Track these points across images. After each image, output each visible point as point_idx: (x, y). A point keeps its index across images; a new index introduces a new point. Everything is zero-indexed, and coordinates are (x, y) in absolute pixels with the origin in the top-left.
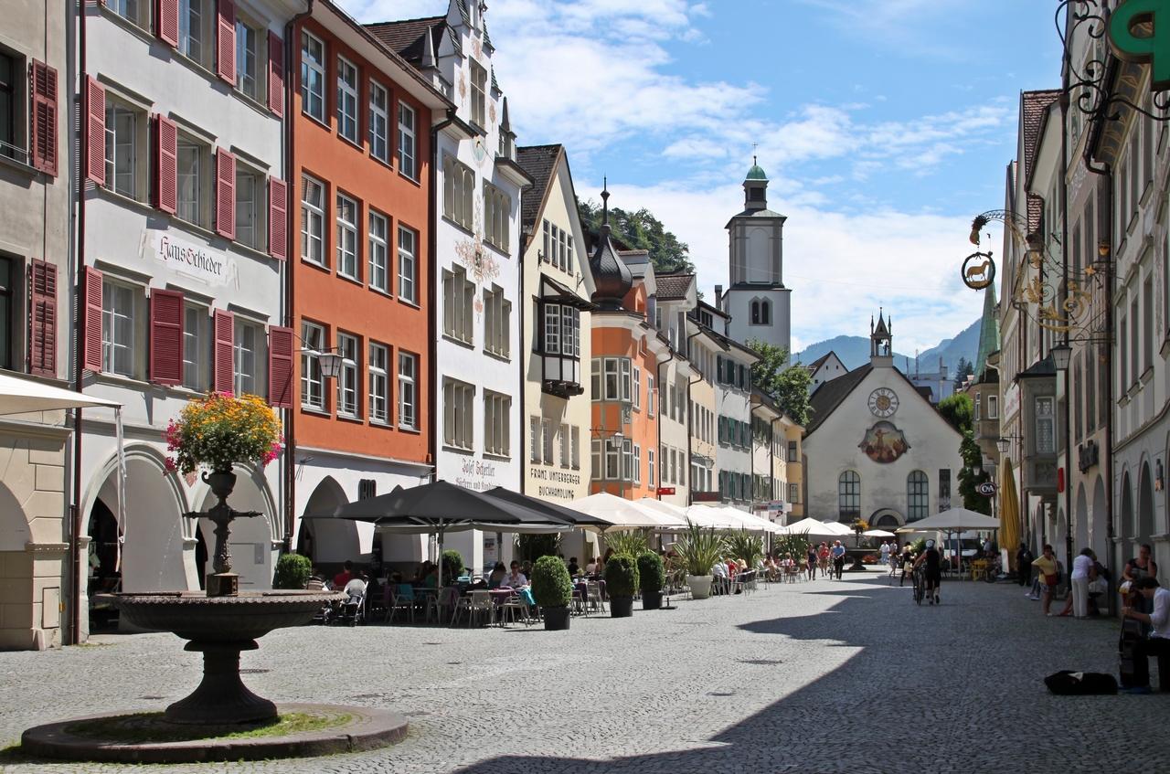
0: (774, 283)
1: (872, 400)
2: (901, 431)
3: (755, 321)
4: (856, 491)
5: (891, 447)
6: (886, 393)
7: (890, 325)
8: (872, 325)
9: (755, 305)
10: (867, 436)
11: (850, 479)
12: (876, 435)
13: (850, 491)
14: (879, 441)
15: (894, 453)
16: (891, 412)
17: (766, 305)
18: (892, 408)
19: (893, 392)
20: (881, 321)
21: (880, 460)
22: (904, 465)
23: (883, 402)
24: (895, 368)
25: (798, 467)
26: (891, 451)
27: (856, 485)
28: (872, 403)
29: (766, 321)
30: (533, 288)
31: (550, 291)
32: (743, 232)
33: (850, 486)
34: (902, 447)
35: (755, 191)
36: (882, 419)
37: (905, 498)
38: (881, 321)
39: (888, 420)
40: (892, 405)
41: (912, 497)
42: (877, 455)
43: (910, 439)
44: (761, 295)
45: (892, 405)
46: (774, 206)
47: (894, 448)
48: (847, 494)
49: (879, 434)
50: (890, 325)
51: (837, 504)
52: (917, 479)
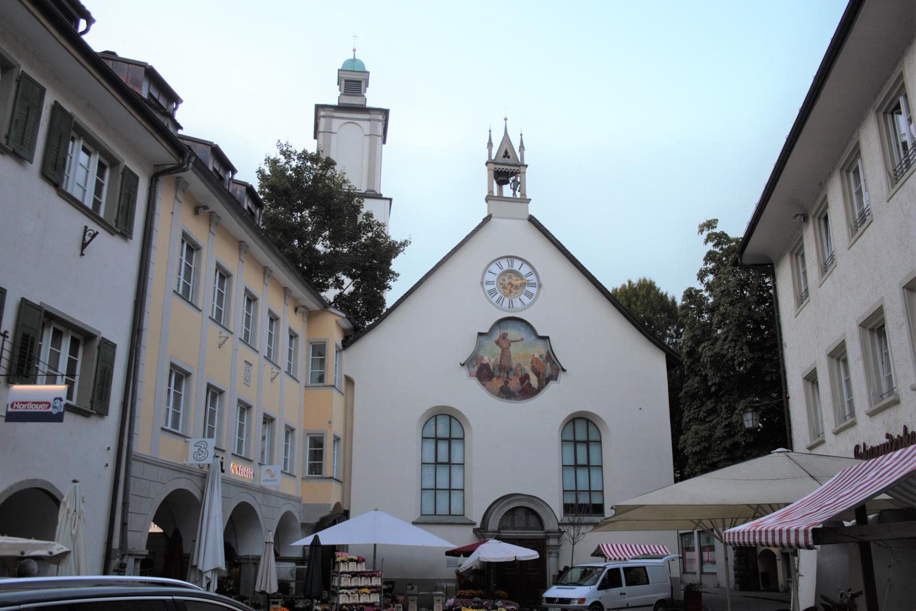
1: (489, 277)
2: (546, 338)
4: (456, 458)
5: (528, 369)
6: (517, 265)
7: (522, 147)
8: (490, 144)
10: (479, 346)
12: (497, 343)
13: (443, 457)
14: (502, 355)
15: (534, 381)
18: (529, 295)
20: (506, 139)
21: (506, 393)
22: (555, 403)
23: (512, 283)
24: (532, 220)
26: (527, 377)
27: (456, 447)
28: (488, 283)
34: (549, 370)
35: (353, 81)
38: (506, 139)
41: (570, 474)
42: (497, 383)
46: (373, 98)
50: (522, 147)
52: (582, 431)
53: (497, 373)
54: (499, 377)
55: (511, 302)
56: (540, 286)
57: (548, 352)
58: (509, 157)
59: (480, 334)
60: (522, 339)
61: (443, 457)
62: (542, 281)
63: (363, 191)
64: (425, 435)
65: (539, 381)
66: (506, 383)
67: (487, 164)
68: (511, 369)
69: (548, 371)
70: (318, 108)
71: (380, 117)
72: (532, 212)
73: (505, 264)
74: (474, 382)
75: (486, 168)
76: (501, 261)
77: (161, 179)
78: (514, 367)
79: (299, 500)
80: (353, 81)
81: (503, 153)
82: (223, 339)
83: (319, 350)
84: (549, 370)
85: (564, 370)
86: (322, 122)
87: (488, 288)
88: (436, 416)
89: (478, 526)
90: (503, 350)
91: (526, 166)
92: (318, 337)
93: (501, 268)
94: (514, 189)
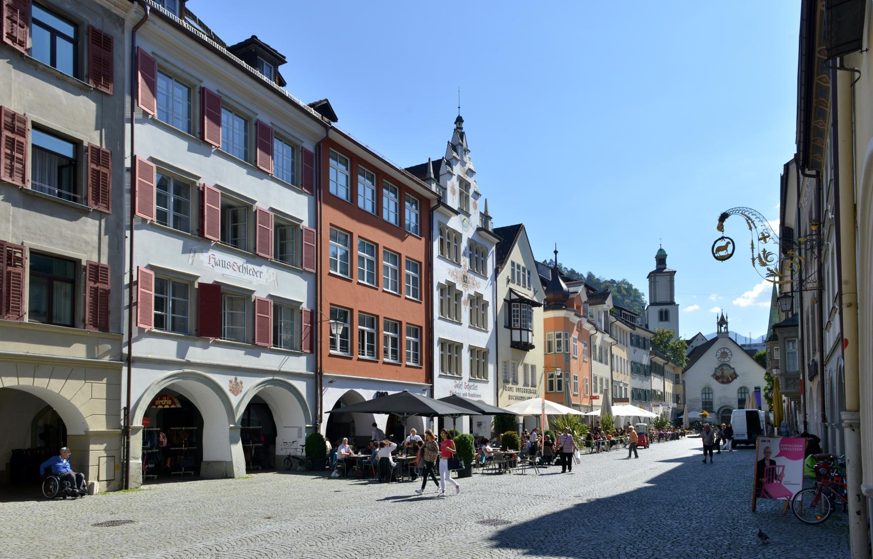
3: (661, 319)
9: (661, 312)
17: (667, 312)
21: (723, 382)
22: (736, 384)
23: (724, 354)
25: (681, 387)
29: (667, 319)
30: (503, 294)
31: (514, 297)
32: (655, 279)
34: (735, 376)
35: (661, 259)
43: (738, 373)
44: (664, 308)
46: (670, 266)
49: (722, 370)
74: (715, 381)
80: (661, 259)
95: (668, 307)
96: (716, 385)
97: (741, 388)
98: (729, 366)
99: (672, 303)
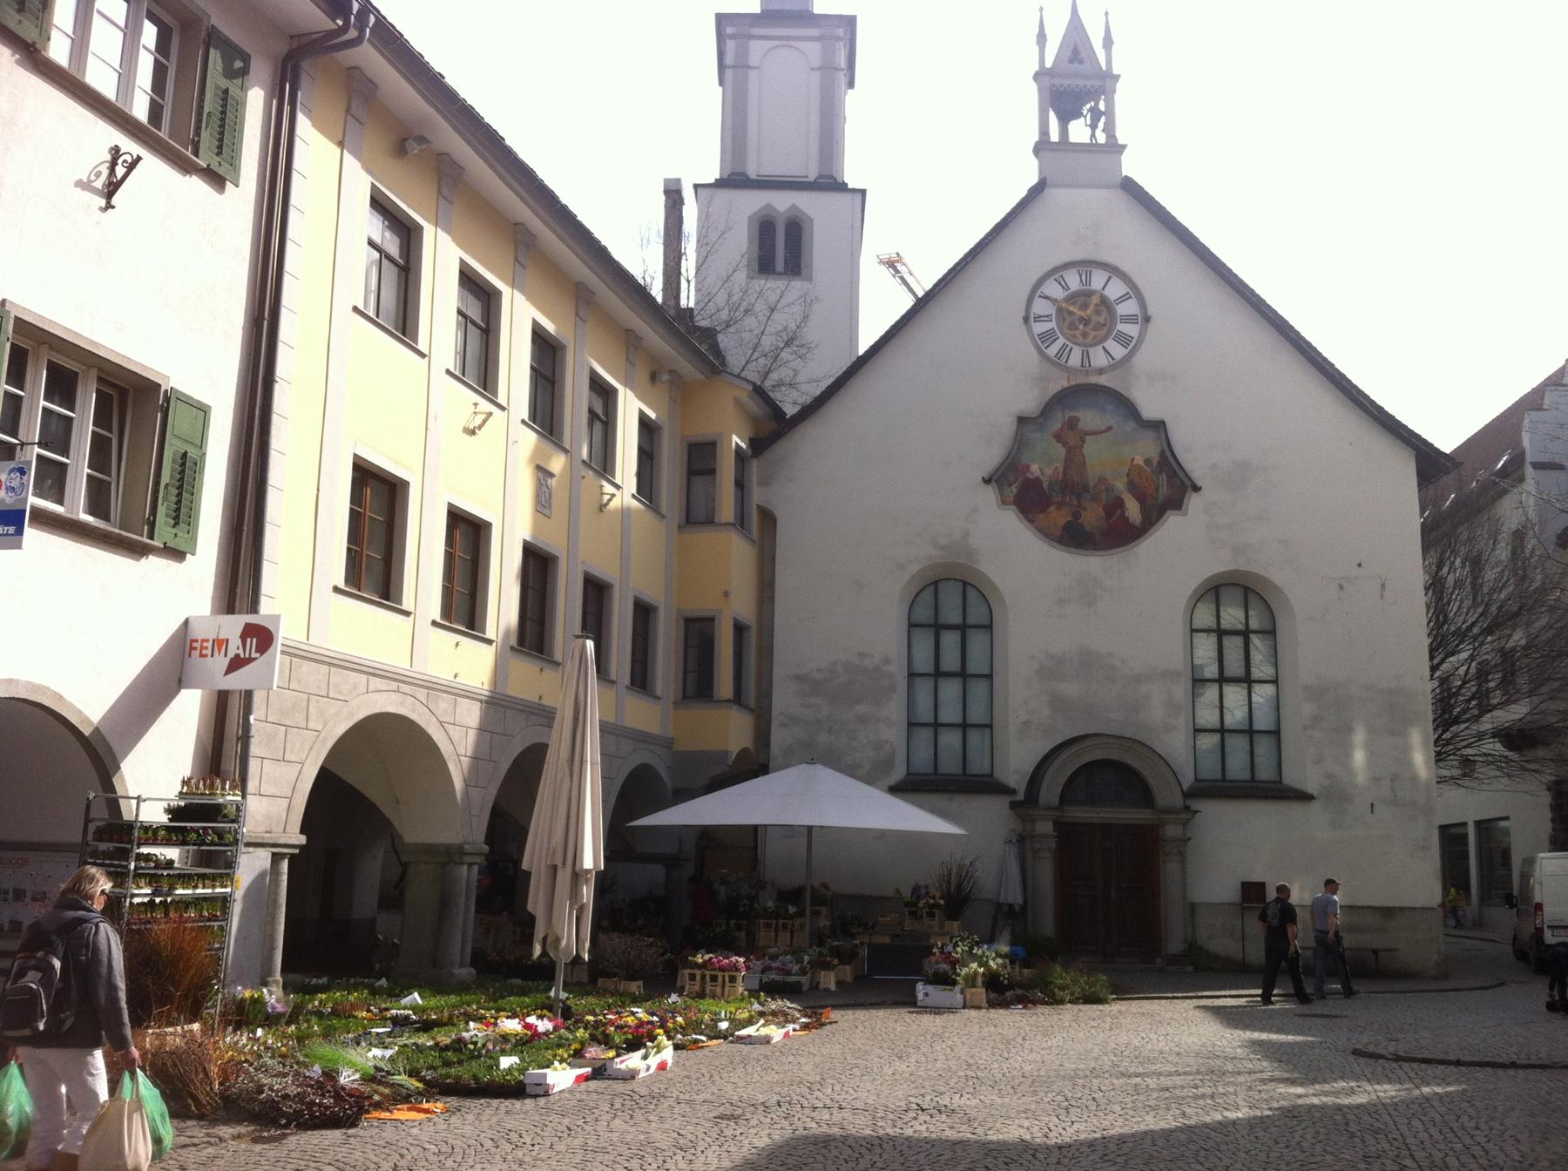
0: (820, 177)
1: (1040, 307)
2: (1159, 426)
4: (976, 664)
5: (1120, 486)
6: (1098, 280)
8: (1042, 38)
9: (765, 228)
11: (951, 615)
12: (1058, 437)
13: (950, 661)
14: (1068, 460)
15: (1133, 510)
16: (1118, 351)
17: (796, 230)
18: (1124, 339)
19: (1125, 277)
20: (1076, 26)
21: (1074, 538)
24: (1131, 188)
26: (1119, 503)
28: (1038, 319)
32: (743, 53)
33: (950, 640)
34: (1167, 487)
36: (1081, 380)
37: (1181, 690)
38: (1076, 26)
39: (1103, 380)
40: (1121, 327)
42: (1058, 518)
43: (1194, 462)
44: (782, 202)
45: (1121, 327)
47: (1132, 488)
48: (938, 674)
50: (1108, 42)
51: (895, 710)
53: (1057, 498)
54: (1060, 506)
55: (1086, 356)
56: (1147, 319)
57: (1162, 453)
58: (1081, 62)
59: (1022, 420)
60: (1109, 429)
61: (950, 661)
62: (1152, 310)
63: (811, 178)
64: (916, 619)
65: (1144, 510)
66: (1077, 515)
67: (1036, 77)
68: (1086, 489)
69: (1164, 491)
70: (722, 20)
71: (841, 32)
72: (1127, 171)
73: (1074, 281)
75: (1034, 87)
76: (1064, 273)
77: (306, 65)
78: (1091, 484)
79: (668, 744)
81: (1069, 53)
82: (479, 420)
83: (701, 458)
84: (1167, 487)
85: (1196, 489)
86: (730, 45)
87: (1039, 328)
88: (936, 583)
89: (1020, 797)
90: (1070, 450)
91: (1117, 77)
92: (702, 430)
93: (1066, 288)
94: (1093, 126)
95: (807, 203)
96: (1017, 557)
97: (1214, 590)
98: (1128, 408)
99: (831, 184)
